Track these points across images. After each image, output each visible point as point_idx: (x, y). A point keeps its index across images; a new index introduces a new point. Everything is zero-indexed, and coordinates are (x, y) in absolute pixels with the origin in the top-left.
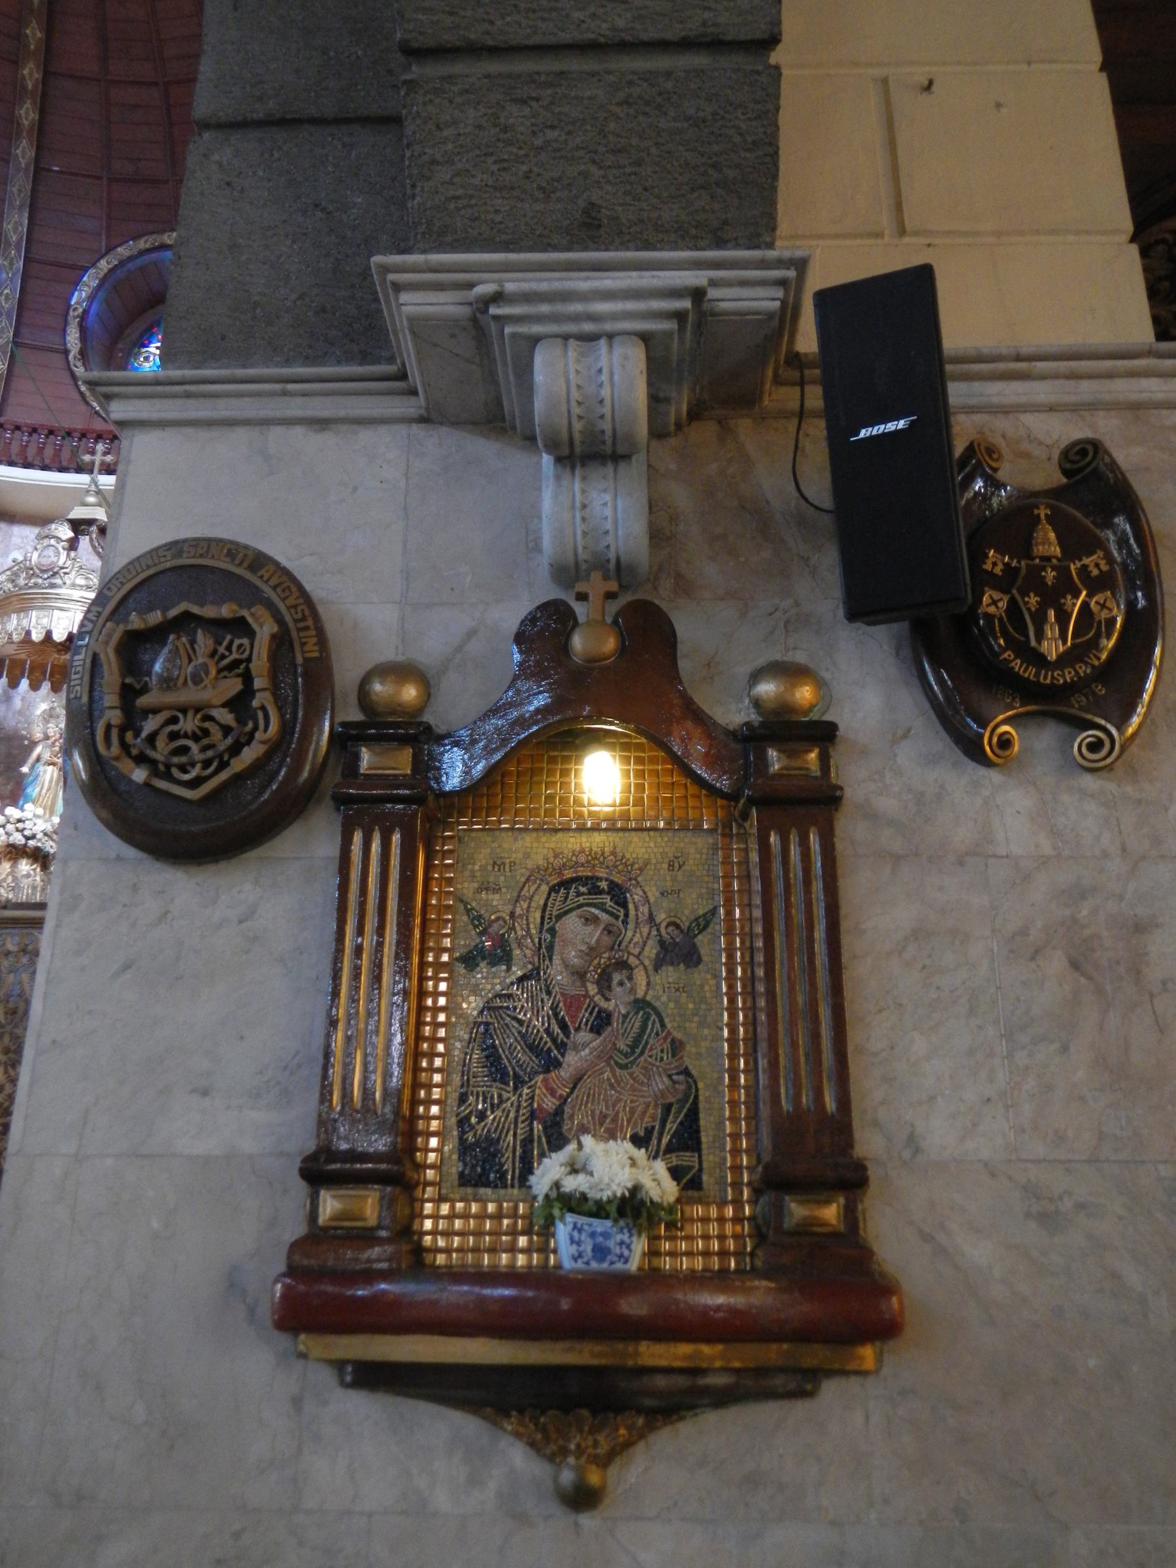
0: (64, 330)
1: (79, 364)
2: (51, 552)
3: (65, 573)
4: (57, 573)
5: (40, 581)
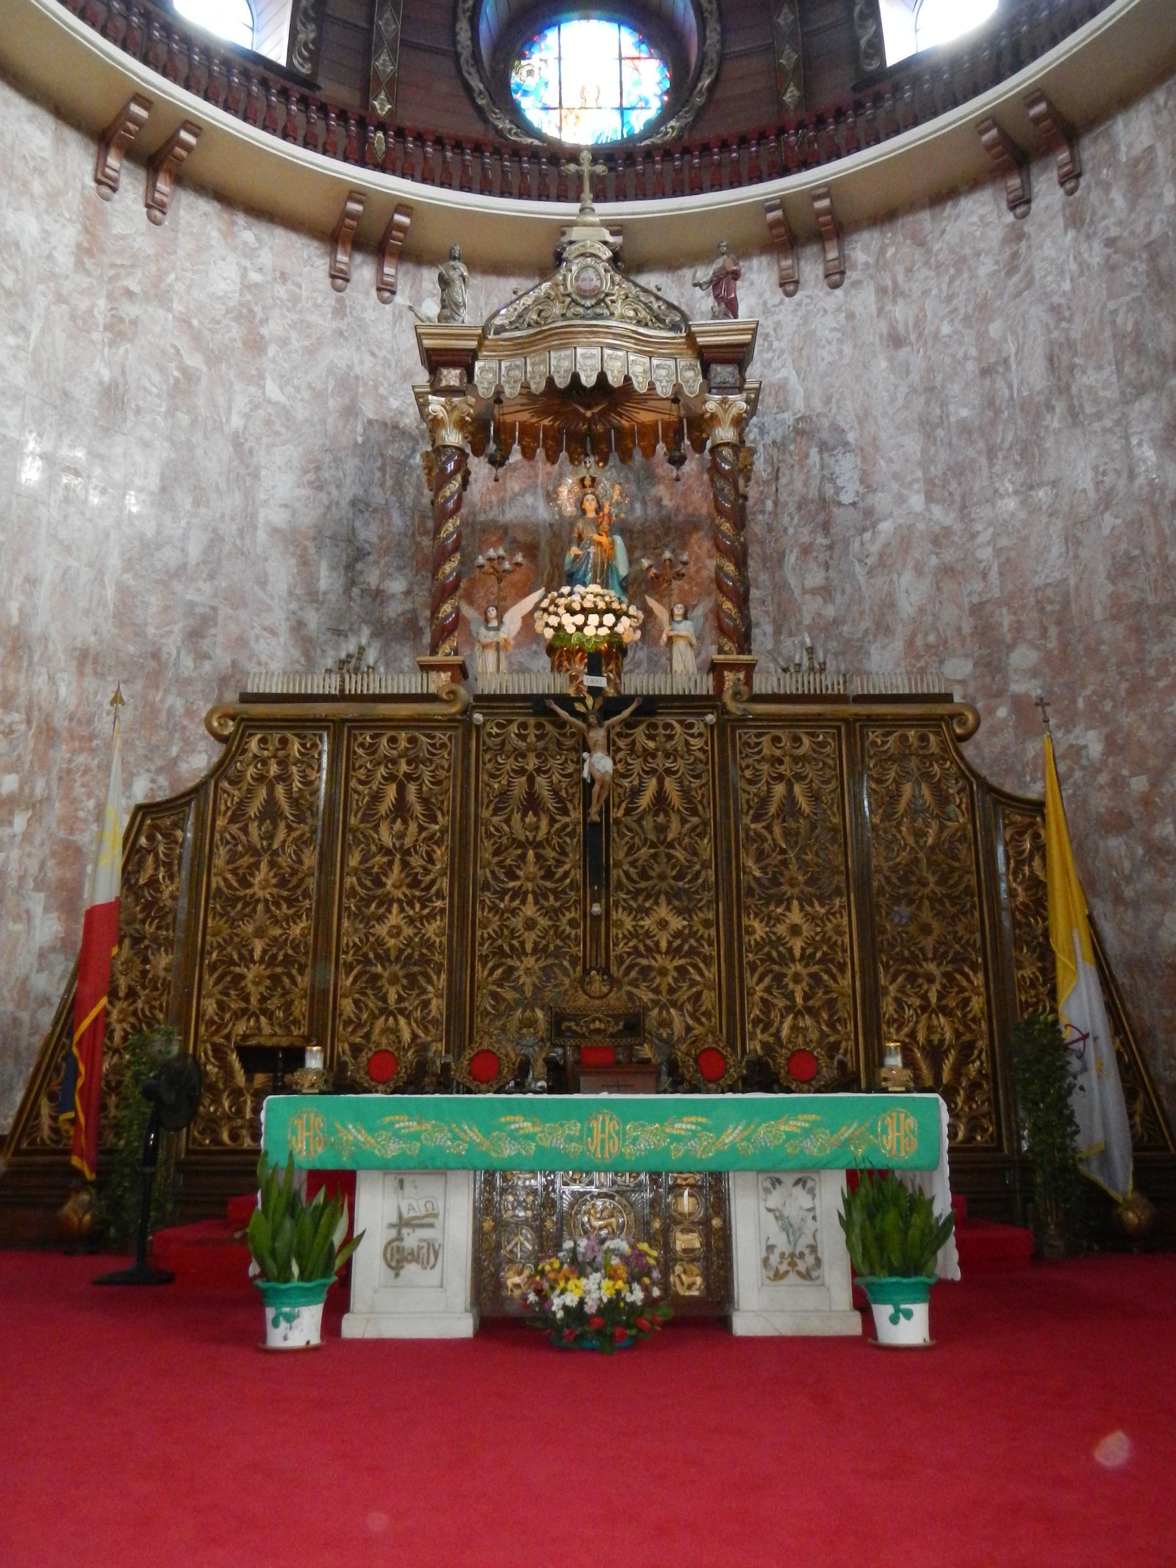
0: (454, 25)
1: (473, 70)
2: (591, 273)
3: (613, 302)
4: (603, 300)
5: (581, 310)
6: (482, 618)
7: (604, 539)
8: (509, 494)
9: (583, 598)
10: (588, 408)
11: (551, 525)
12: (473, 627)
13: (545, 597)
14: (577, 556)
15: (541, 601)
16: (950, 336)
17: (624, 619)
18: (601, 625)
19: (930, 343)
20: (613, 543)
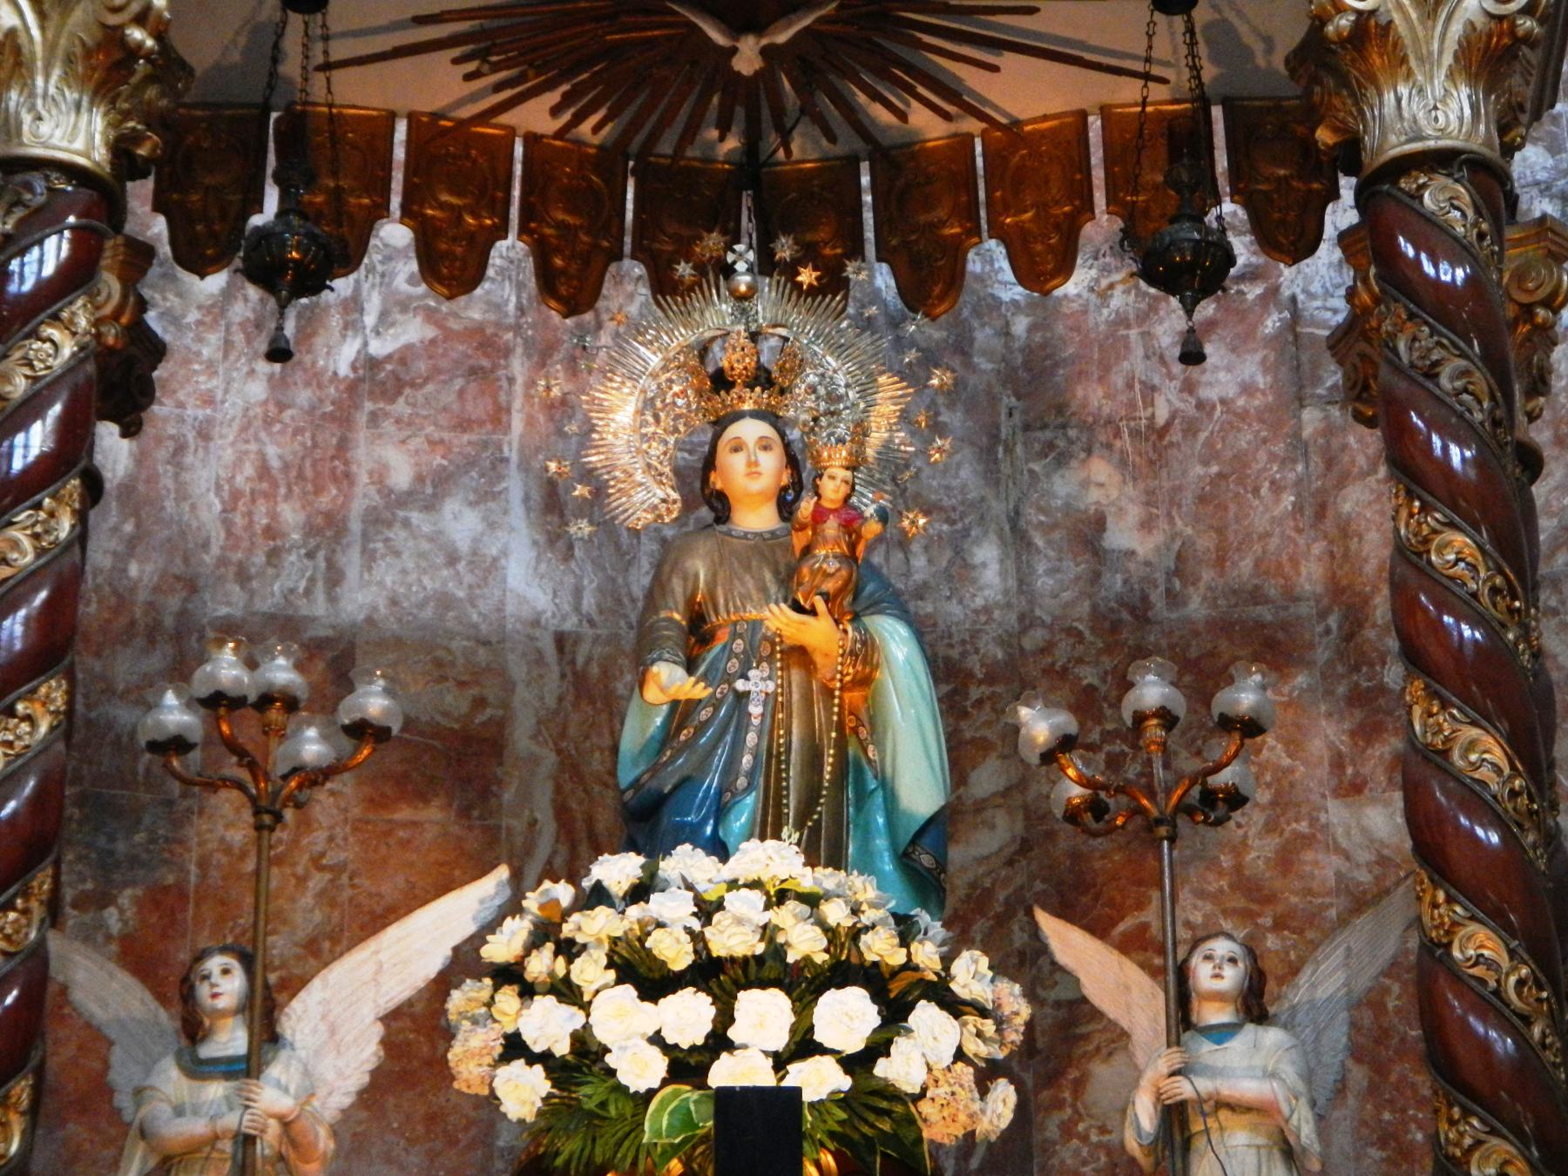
6: (167, 1020)
7: (819, 633)
8: (364, 497)
9: (707, 910)
10: (740, 25)
11: (562, 641)
12: (122, 1074)
13: (513, 907)
14: (681, 712)
15: (492, 926)
17: (926, 1015)
18: (804, 1045)
20: (866, 653)
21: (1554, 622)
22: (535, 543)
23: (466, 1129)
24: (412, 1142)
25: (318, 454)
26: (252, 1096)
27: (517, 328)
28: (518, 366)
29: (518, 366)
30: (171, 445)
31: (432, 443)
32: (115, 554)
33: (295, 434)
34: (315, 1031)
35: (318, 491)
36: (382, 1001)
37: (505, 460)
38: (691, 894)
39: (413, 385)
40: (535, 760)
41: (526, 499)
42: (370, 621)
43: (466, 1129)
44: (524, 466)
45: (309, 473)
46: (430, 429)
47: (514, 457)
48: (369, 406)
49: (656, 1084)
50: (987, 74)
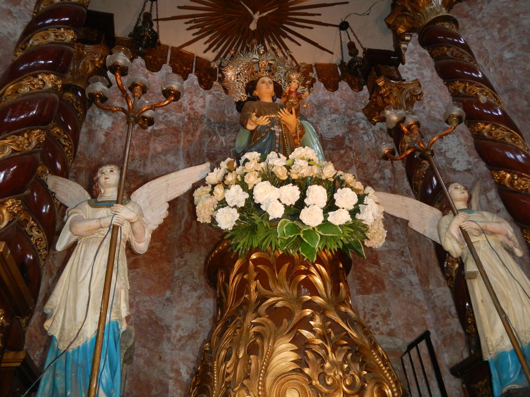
8: (151, 153)
16: (514, 59)
19: (497, 64)
21: (376, 185)
22: (185, 163)
23: (168, 272)
24: (156, 274)
25: (143, 144)
26: (118, 210)
27: (182, 128)
28: (182, 134)
29: (182, 134)
30: (113, 139)
31: (166, 145)
32: (99, 156)
33: (139, 140)
34: (144, 202)
35: (143, 150)
36: (168, 196)
37: (180, 149)
38: (247, 196)
39: (162, 135)
40: (184, 201)
41: (183, 156)
42: (152, 173)
43: (168, 272)
44: (183, 150)
45: (141, 147)
46: (165, 142)
47: (181, 149)
48: (153, 137)
49: (280, 217)
50: (310, 30)
